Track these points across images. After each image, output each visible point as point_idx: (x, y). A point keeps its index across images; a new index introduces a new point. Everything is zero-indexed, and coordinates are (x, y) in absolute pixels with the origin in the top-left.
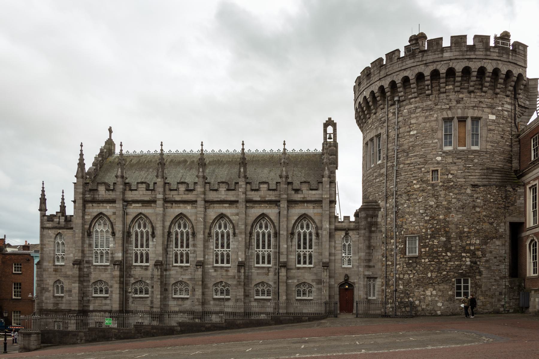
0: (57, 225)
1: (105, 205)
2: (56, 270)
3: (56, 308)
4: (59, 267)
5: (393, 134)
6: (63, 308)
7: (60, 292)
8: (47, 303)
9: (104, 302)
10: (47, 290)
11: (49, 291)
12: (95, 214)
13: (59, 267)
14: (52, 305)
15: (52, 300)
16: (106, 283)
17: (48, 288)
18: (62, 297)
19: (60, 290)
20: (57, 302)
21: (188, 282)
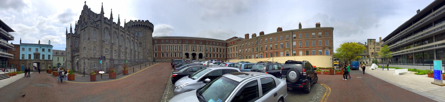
0: (94, 26)
1: (108, 25)
2: (94, 43)
3: (94, 57)
4: (95, 42)
5: (145, 33)
6: (96, 57)
7: (94, 51)
8: (91, 55)
9: (108, 56)
10: (91, 50)
11: (92, 50)
12: (105, 27)
13: (95, 42)
14: (93, 56)
15: (93, 54)
16: (108, 50)
17: (92, 49)
18: (96, 53)
19: (94, 50)
20: (94, 55)
21: (123, 52)
